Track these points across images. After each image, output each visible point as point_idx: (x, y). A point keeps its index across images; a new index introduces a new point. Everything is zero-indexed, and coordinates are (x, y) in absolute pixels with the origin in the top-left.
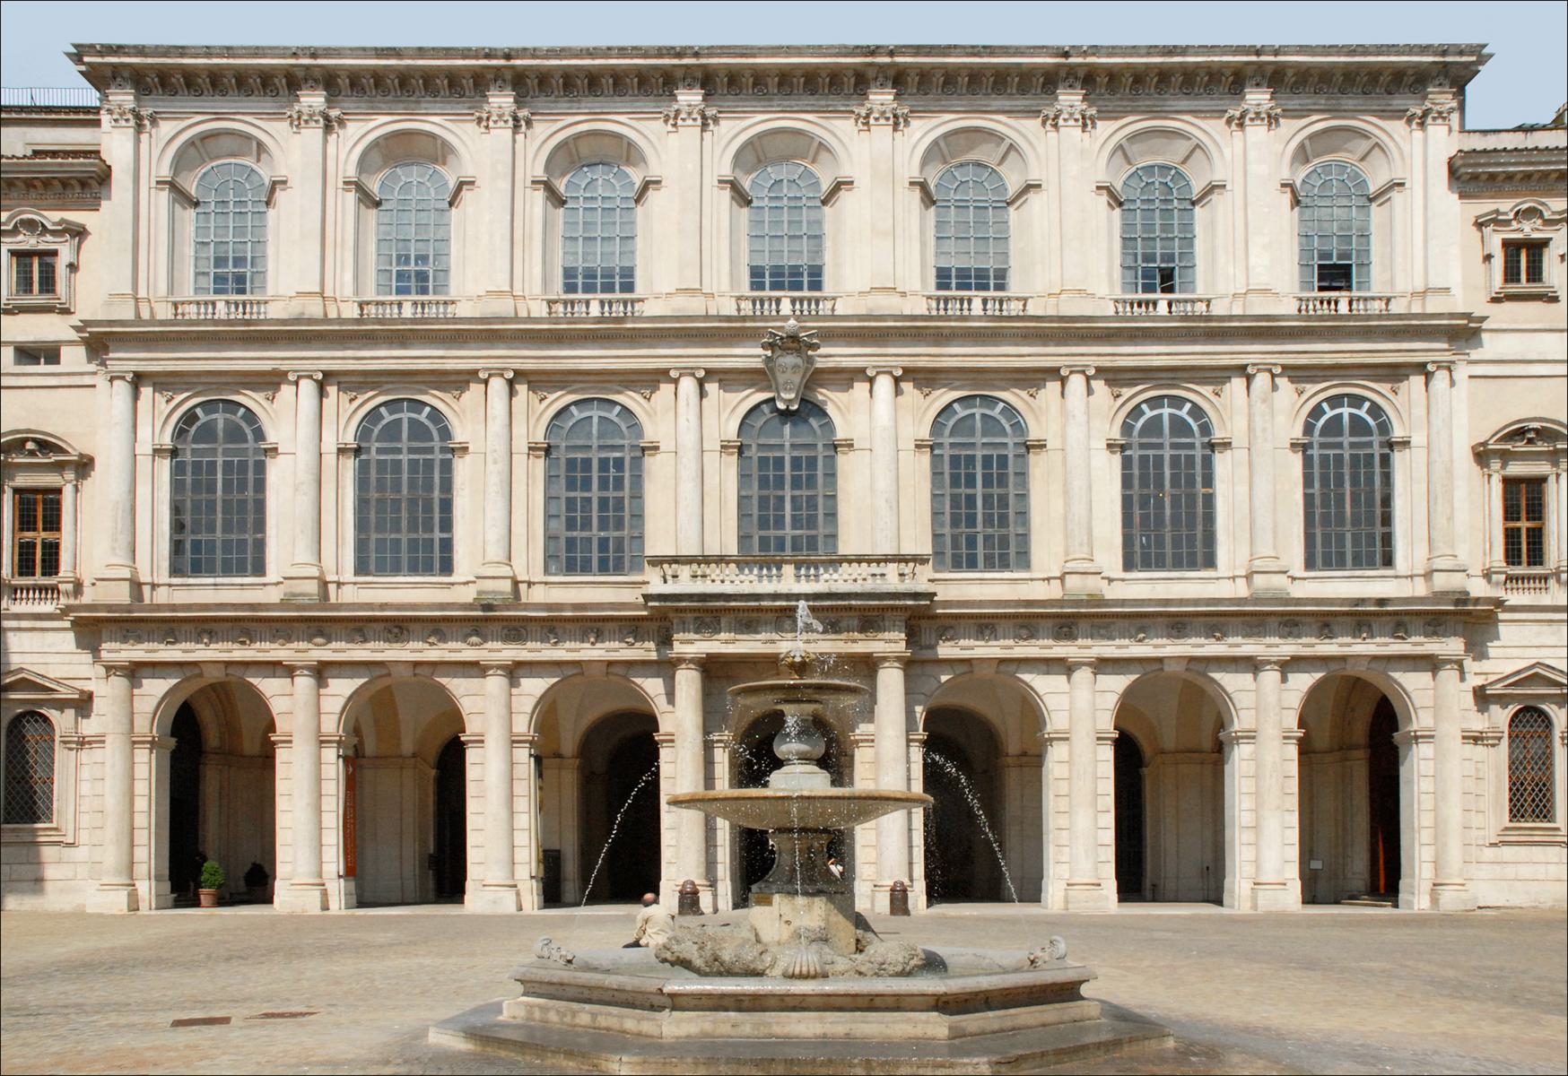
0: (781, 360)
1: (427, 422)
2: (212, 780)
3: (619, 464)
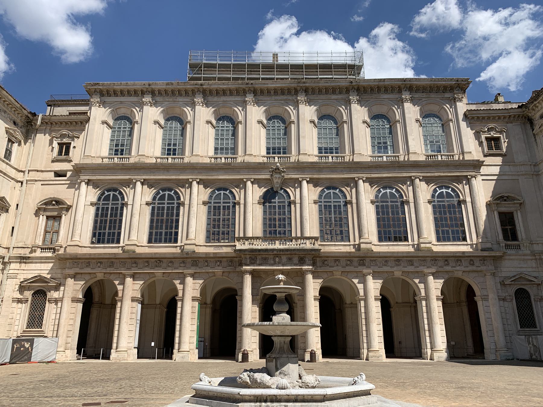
0: (275, 176)
1: (173, 195)
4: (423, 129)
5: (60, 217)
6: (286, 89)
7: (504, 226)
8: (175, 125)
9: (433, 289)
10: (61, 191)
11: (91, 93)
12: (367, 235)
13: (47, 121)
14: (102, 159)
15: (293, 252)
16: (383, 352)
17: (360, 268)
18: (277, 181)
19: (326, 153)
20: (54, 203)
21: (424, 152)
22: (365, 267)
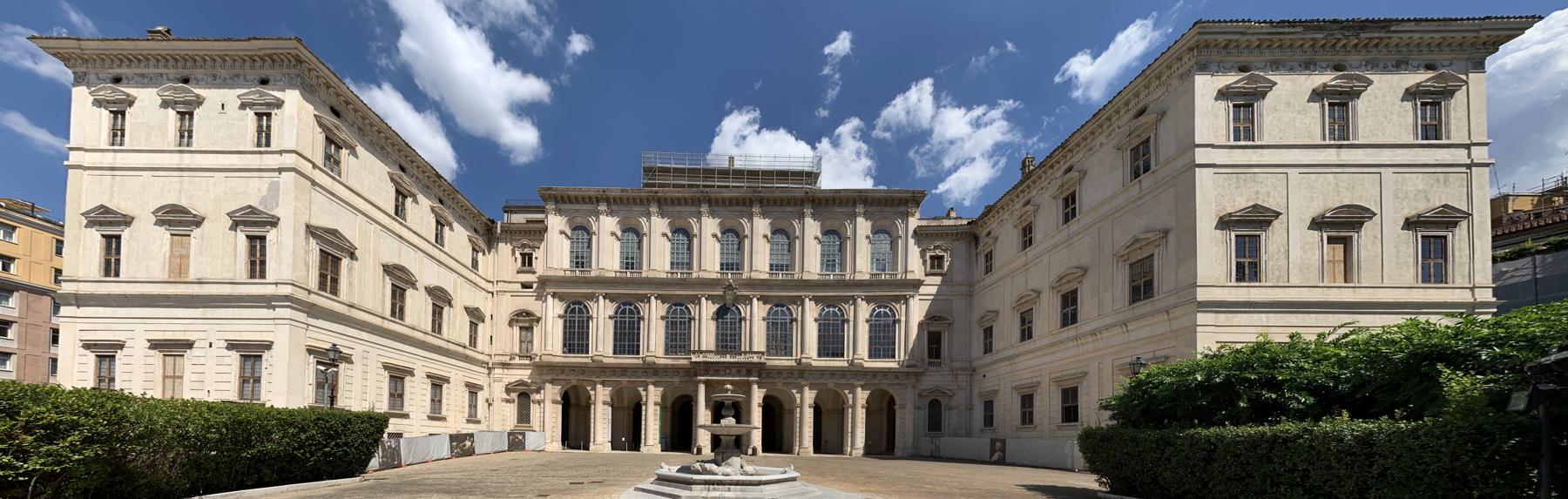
8: (632, 236)
10: (529, 303)
18: (729, 297)
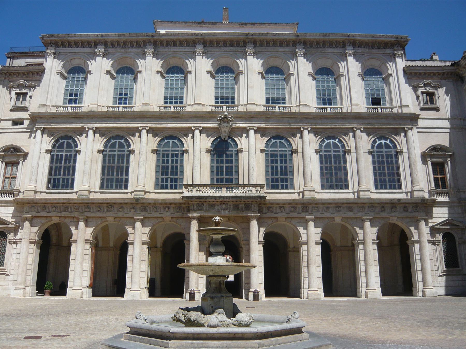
0: (223, 125)
1: (124, 143)
2: (52, 254)
3: (177, 155)
4: (365, 83)
5: (18, 163)
6: (235, 41)
7: (436, 175)
9: (370, 233)
10: (20, 139)
11: (47, 44)
12: (310, 183)
13: (5, 72)
14: (57, 107)
15: (239, 200)
16: (321, 291)
17: (303, 215)
18: (225, 130)
19: (272, 103)
20: (12, 150)
21: (365, 105)
22: (307, 214)
